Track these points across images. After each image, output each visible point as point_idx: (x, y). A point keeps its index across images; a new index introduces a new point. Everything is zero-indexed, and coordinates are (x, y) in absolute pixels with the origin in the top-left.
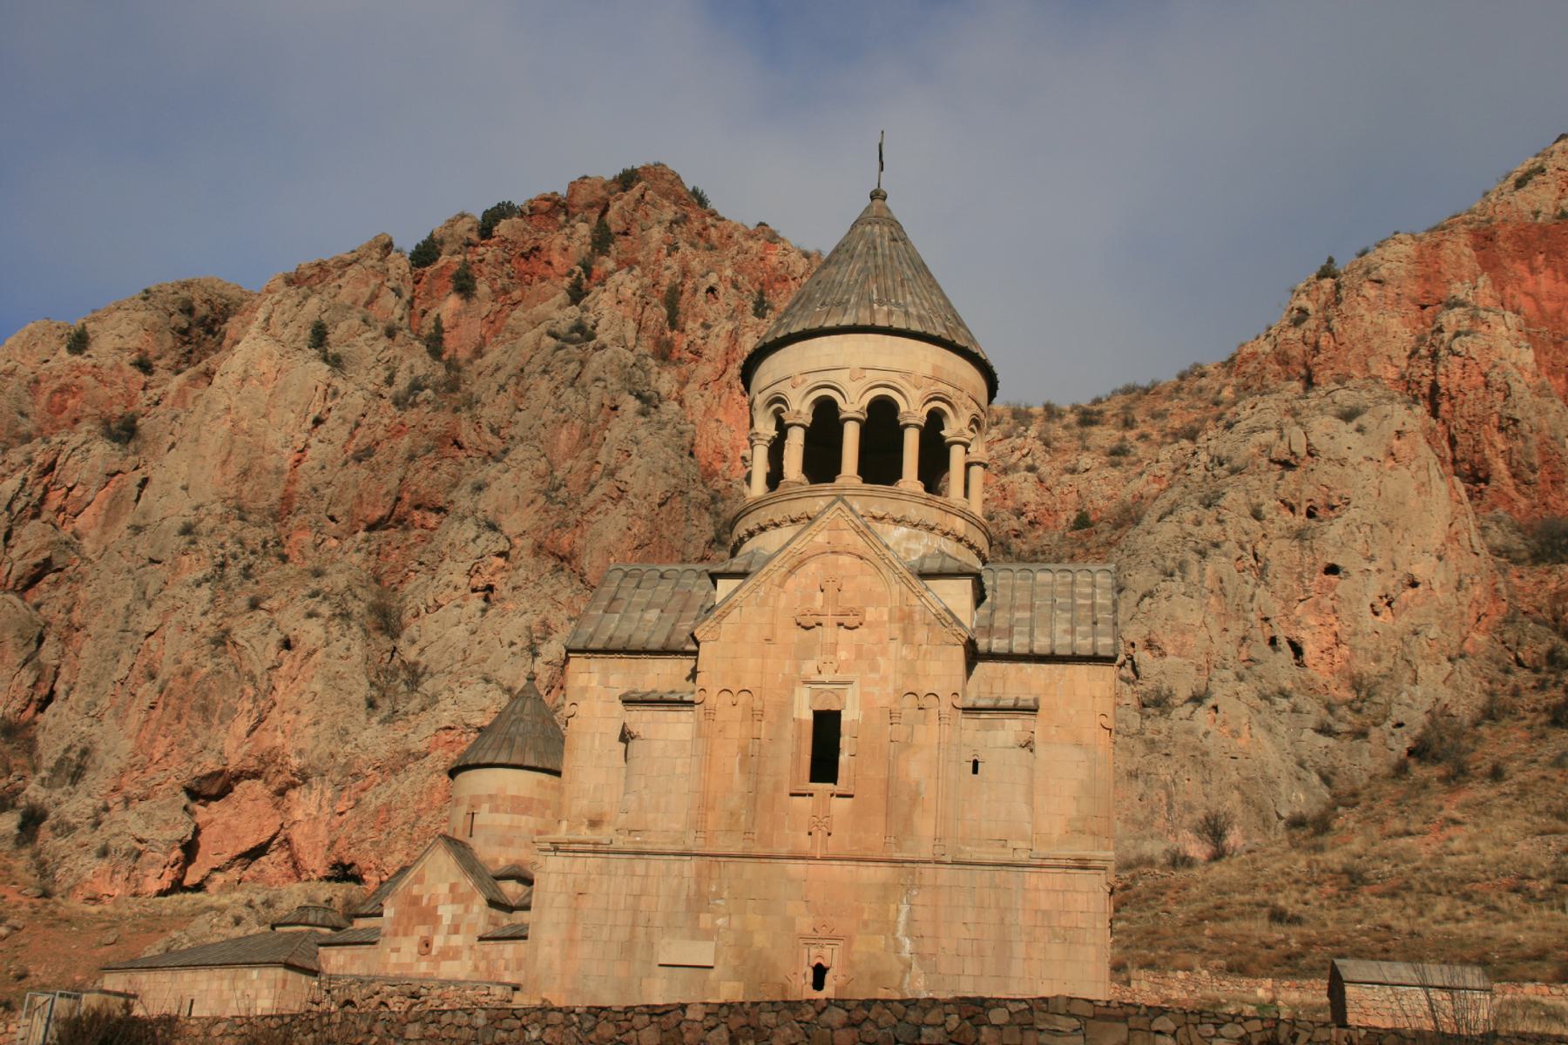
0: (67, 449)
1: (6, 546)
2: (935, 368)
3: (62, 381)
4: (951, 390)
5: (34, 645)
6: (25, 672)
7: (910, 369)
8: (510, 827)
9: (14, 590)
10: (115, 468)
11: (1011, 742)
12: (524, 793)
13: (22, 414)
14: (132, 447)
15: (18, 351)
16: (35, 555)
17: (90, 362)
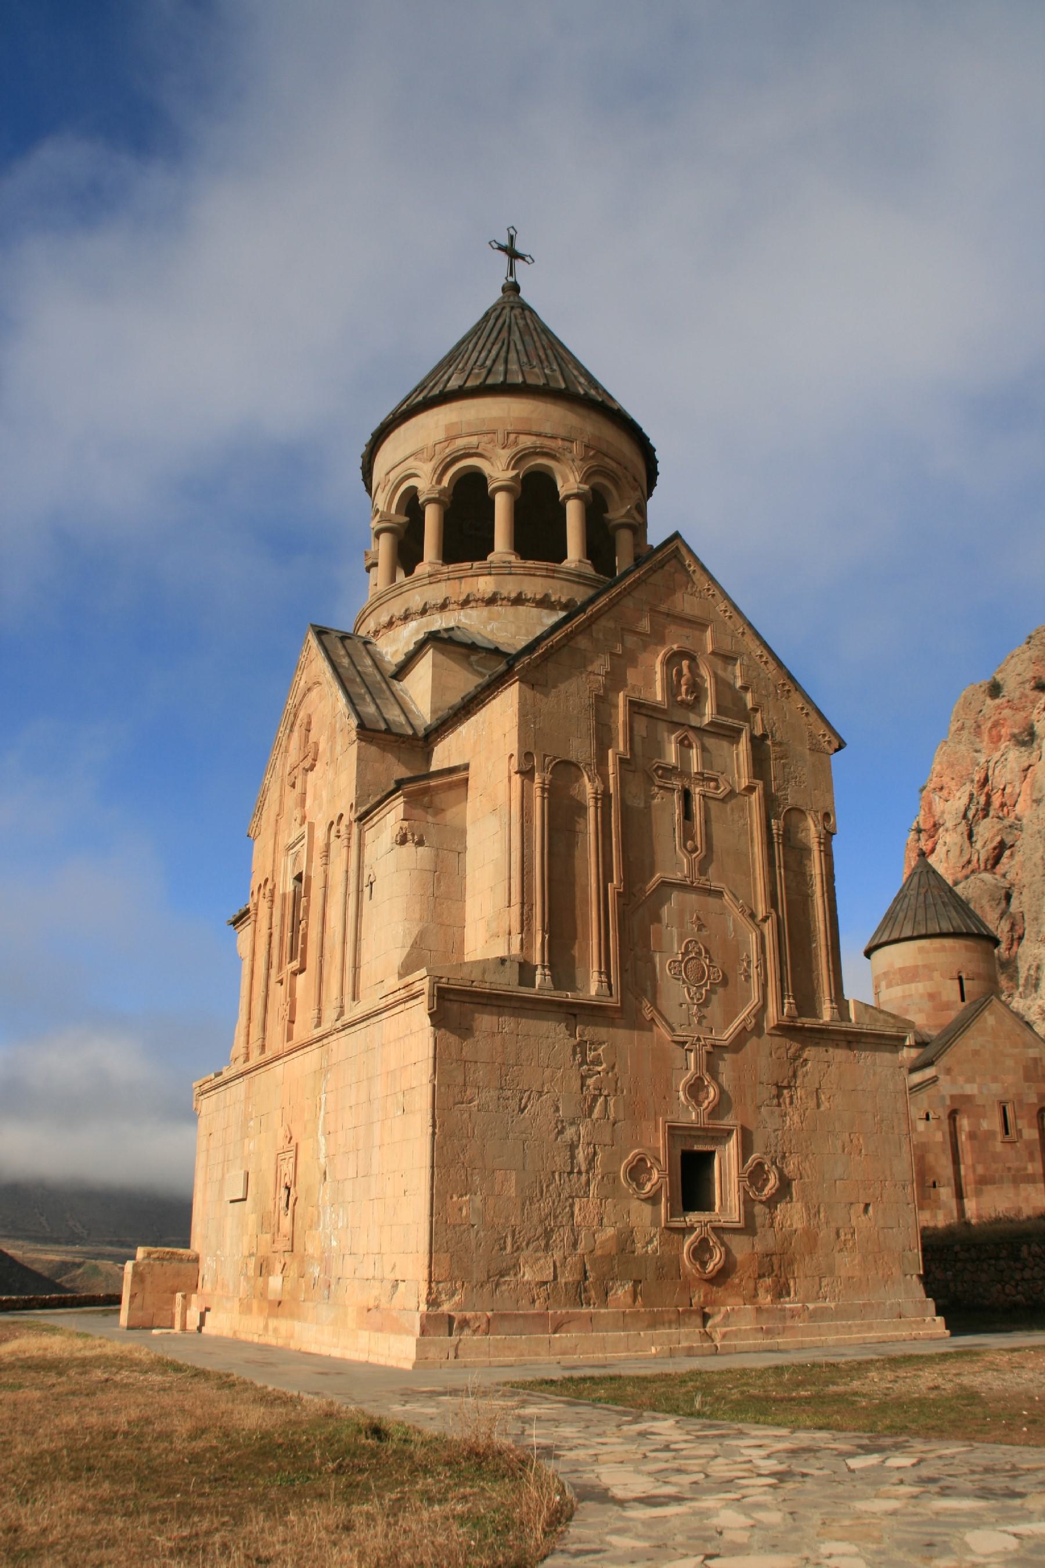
0: (991, 764)
1: (971, 843)
2: (448, 428)
3: (992, 720)
4: (474, 440)
5: (1003, 904)
6: (1003, 922)
7: (420, 445)
8: (904, 997)
9: (986, 870)
10: (1026, 764)
11: (389, 846)
12: (909, 963)
13: (977, 751)
14: (1035, 745)
15: (961, 712)
16: (992, 841)
17: (1004, 700)
